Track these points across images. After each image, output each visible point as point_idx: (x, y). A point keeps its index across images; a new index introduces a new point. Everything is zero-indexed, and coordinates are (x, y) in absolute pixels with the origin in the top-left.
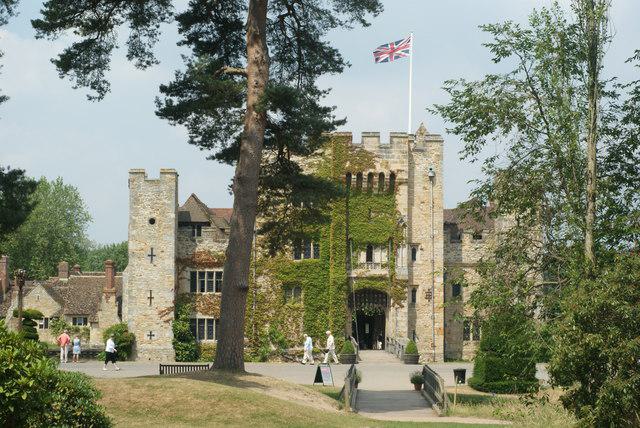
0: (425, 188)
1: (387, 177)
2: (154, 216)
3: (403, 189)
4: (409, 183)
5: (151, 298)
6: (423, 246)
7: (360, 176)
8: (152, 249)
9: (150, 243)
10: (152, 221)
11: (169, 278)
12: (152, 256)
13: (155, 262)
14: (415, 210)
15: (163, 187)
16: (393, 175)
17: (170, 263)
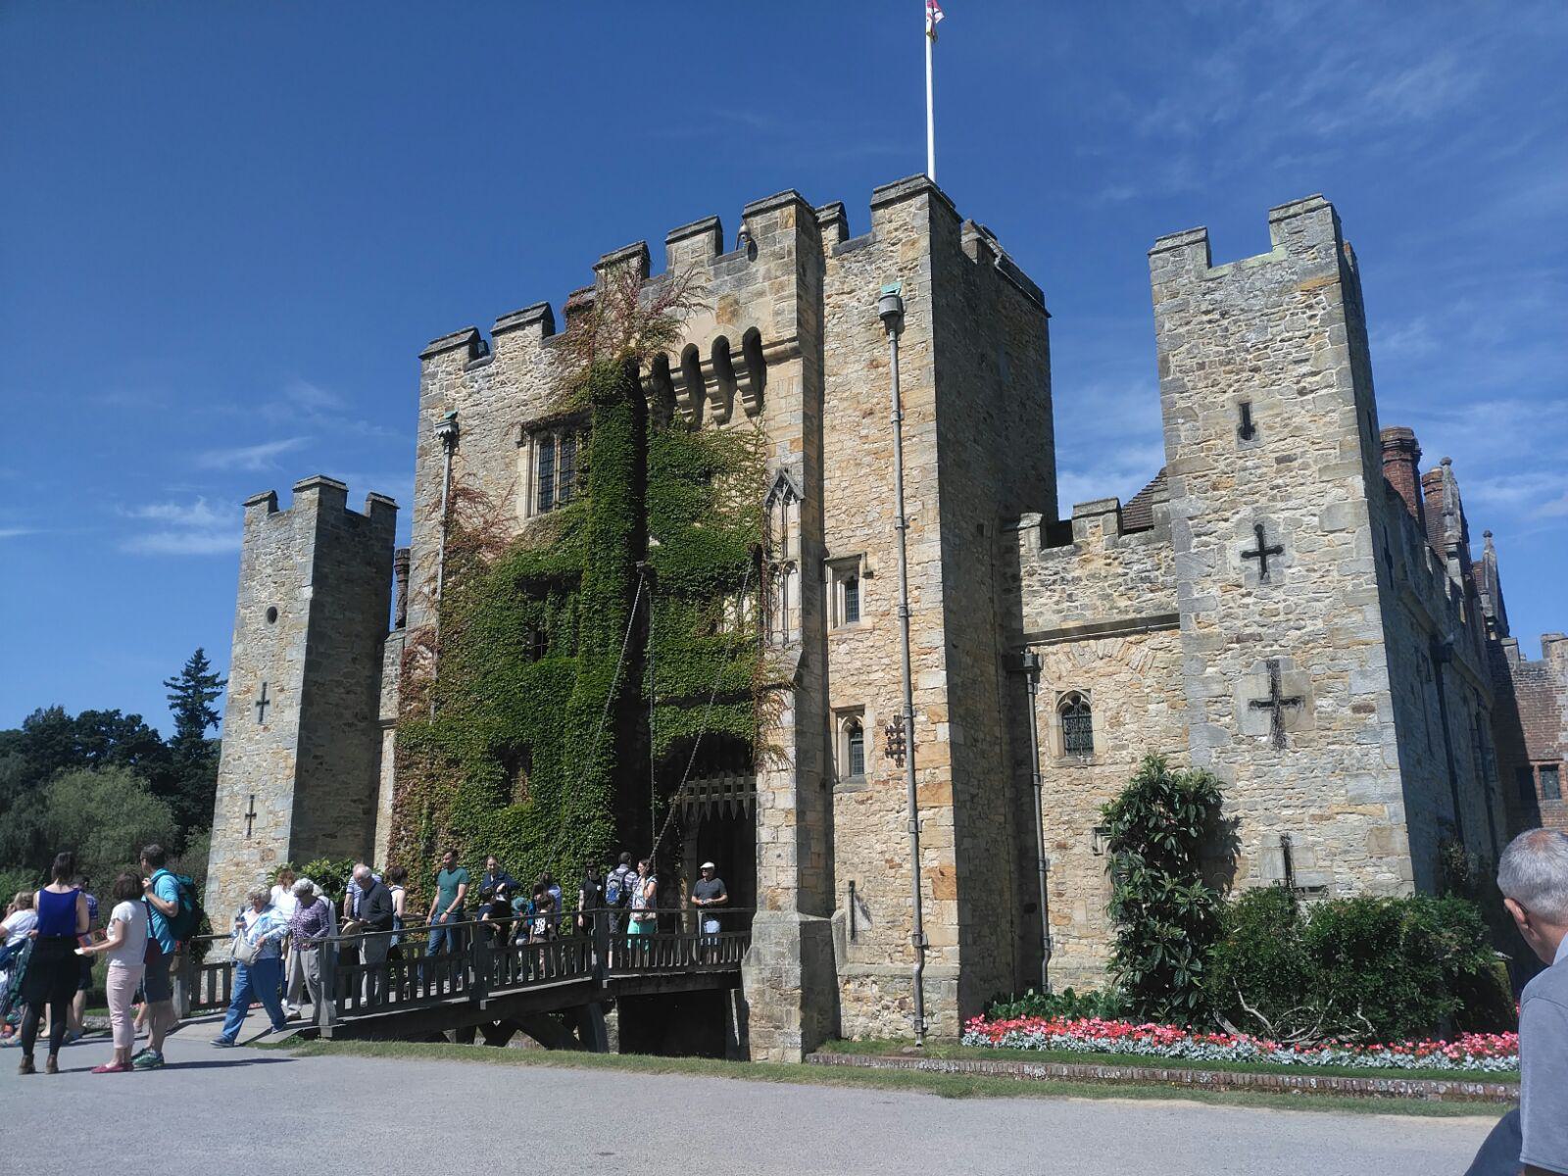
0: (874, 364)
1: (736, 345)
2: (275, 601)
3: (785, 380)
4: (810, 344)
5: (251, 816)
6: (873, 562)
7: (661, 362)
8: (265, 685)
9: (265, 674)
10: (272, 615)
11: (288, 756)
12: (263, 703)
13: (266, 720)
14: (836, 444)
15: (298, 522)
16: (753, 339)
17: (292, 716)
